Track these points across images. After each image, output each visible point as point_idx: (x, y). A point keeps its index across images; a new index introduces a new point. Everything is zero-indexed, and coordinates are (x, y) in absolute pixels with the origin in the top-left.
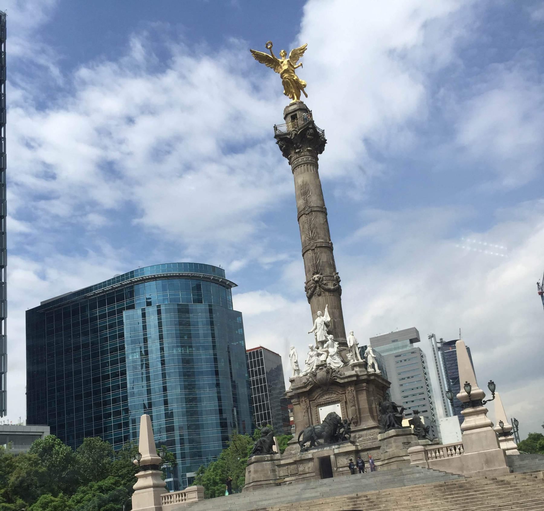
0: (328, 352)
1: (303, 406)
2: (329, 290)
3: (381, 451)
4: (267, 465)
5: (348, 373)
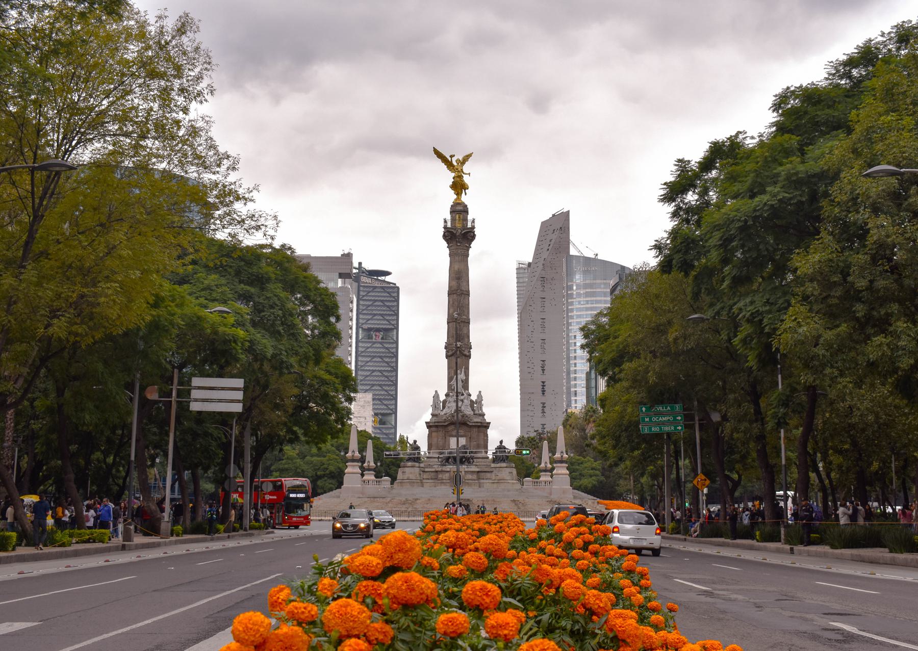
0: (462, 401)
1: (441, 434)
2: (465, 356)
3: (493, 474)
4: (417, 470)
5: (476, 420)
